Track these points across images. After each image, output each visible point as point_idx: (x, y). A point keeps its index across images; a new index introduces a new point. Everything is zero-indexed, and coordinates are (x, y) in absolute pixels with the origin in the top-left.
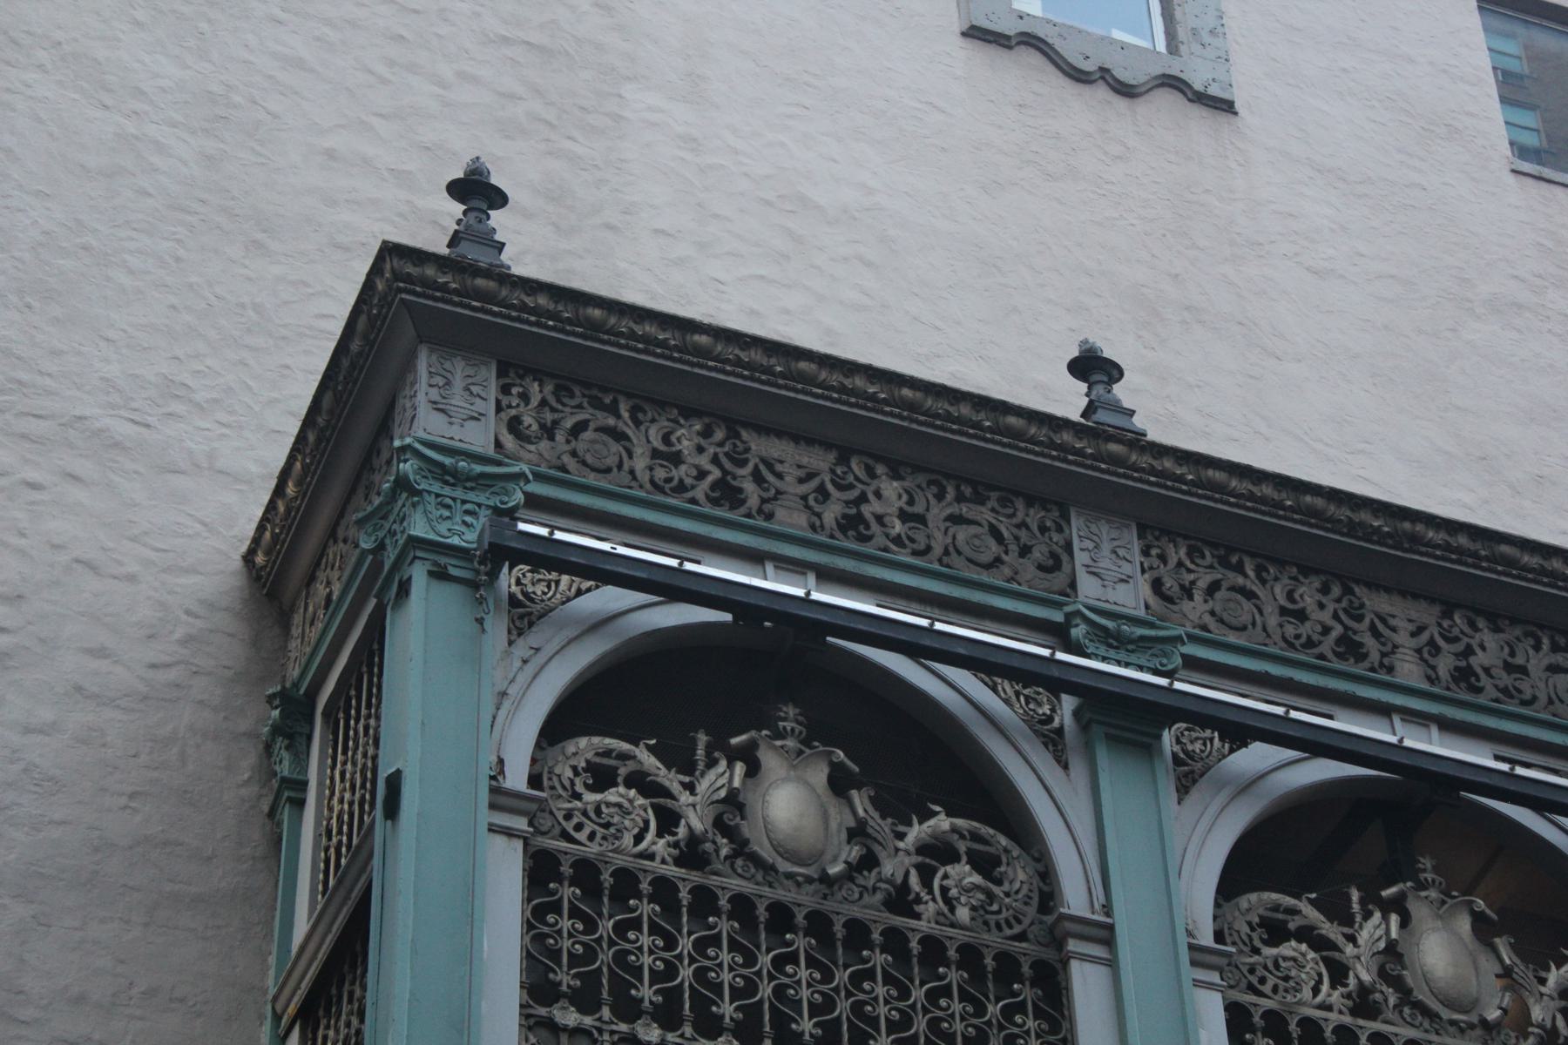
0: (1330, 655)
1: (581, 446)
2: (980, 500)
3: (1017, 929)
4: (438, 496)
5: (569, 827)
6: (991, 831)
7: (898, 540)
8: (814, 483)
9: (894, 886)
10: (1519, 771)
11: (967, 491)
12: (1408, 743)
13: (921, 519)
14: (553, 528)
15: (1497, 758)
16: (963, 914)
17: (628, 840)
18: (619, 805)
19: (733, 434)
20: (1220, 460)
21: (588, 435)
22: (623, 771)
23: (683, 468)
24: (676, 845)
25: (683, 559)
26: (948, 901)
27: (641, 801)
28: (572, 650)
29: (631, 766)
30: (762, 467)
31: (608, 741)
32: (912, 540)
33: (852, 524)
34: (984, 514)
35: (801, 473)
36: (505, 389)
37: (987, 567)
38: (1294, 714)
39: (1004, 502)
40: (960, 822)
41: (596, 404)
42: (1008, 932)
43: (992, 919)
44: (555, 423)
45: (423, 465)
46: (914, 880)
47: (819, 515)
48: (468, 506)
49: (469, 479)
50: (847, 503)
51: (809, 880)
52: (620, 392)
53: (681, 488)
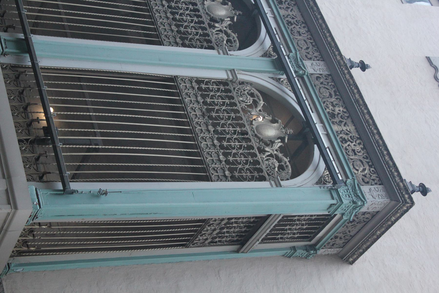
0: (290, 29)
3: (270, 174)
5: (236, 89)
6: (290, 169)
7: (346, 149)
8: (349, 133)
10: (277, 36)
11: (370, 164)
12: (317, 125)
15: (275, 28)
16: (267, 162)
17: (241, 99)
18: (247, 97)
19: (348, 117)
21: (327, 91)
22: (255, 98)
23: (332, 107)
24: (245, 108)
25: (307, 99)
26: (267, 160)
27: (251, 102)
28: (271, 80)
29: (258, 100)
32: (349, 152)
33: (344, 140)
34: (367, 168)
35: (349, 130)
36: (325, 76)
38: (306, 102)
40: (288, 163)
41: (335, 92)
42: (268, 172)
44: (325, 84)
45: (353, 184)
46: (267, 154)
47: (341, 133)
49: (356, 194)
50: (348, 139)
51: (254, 132)
52: (308, 26)
53: (328, 107)
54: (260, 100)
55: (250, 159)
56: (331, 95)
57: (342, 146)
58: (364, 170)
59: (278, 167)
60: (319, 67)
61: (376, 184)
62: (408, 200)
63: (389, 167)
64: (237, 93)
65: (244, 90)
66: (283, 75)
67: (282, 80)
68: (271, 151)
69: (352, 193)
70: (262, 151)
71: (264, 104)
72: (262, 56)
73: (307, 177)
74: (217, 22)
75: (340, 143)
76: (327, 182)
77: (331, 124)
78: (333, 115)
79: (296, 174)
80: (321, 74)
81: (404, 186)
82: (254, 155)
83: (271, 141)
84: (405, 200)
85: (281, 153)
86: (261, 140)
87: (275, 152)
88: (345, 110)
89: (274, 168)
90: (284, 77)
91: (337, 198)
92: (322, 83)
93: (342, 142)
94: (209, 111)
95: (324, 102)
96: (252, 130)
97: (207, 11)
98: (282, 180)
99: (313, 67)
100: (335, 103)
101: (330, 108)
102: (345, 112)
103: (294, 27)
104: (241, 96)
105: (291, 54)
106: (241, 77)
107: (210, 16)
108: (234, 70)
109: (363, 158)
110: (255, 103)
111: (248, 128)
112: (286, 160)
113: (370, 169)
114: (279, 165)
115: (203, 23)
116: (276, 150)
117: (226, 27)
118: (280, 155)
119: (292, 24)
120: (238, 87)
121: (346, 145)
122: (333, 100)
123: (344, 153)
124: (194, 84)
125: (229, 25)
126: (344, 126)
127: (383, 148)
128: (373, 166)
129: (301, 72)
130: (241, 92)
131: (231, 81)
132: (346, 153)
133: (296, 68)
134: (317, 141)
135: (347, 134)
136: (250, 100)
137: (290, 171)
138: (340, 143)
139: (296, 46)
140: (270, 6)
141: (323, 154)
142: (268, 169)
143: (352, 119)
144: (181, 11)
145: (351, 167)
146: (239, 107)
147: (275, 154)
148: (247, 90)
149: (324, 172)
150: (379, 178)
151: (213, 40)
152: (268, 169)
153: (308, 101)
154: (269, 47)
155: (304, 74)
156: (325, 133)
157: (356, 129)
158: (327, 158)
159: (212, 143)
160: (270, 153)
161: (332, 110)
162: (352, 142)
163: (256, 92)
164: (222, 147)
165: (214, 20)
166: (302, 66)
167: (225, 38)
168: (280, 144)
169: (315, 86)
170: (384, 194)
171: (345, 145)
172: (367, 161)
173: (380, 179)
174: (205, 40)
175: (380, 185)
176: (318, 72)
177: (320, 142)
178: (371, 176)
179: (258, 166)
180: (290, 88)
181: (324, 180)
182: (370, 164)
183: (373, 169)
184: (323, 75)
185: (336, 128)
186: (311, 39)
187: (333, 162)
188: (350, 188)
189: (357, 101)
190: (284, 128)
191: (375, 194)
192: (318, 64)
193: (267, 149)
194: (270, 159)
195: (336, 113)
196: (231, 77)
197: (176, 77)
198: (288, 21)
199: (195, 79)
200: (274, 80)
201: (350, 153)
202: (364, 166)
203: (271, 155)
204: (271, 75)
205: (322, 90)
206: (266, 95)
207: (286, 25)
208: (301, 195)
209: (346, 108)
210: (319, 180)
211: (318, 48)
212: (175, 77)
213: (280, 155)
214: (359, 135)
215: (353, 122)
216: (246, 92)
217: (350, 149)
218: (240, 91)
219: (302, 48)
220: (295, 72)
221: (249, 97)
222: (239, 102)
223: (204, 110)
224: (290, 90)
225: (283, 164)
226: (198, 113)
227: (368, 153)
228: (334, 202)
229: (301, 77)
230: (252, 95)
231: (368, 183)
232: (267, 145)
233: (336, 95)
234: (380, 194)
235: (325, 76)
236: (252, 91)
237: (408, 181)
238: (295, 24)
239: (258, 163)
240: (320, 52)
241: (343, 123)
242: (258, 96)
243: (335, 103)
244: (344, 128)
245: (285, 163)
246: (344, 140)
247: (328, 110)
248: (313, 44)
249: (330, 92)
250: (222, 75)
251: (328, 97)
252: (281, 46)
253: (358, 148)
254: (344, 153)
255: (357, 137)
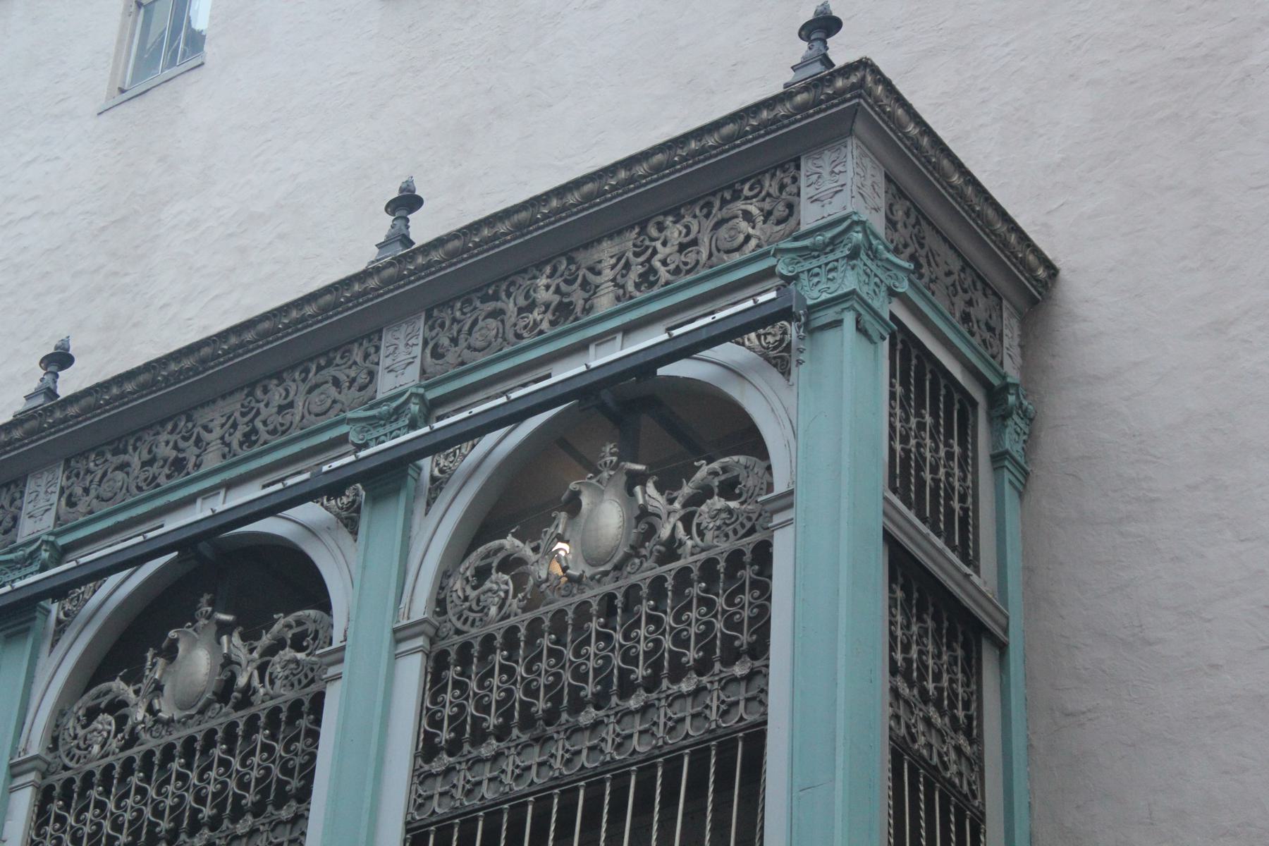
1: (472, 341)
2: (737, 196)
3: (748, 525)
4: (809, 271)
5: (459, 625)
6: (735, 458)
7: (677, 271)
8: (623, 261)
9: (662, 544)
10: (290, 482)
11: (728, 196)
12: (593, 364)
13: (695, 242)
14: (75, 560)
15: (264, 487)
16: (709, 536)
18: (490, 590)
19: (571, 261)
20: (139, 368)
21: (481, 324)
22: (495, 565)
23: (536, 313)
25: (504, 393)
26: (701, 534)
27: (506, 577)
29: (501, 556)
30: (650, 251)
31: (480, 550)
32: (686, 264)
33: (648, 277)
34: (740, 205)
35: (613, 261)
36: (432, 328)
37: (739, 249)
38: (514, 395)
39: (101, 454)
40: (716, 465)
41: (485, 299)
42: (741, 532)
43: (729, 530)
44: (459, 331)
46: (681, 532)
47: (623, 287)
48: (830, 266)
50: (642, 264)
51: (606, 574)
53: (536, 324)
54: (501, 548)
55: (696, 590)
56: (497, 314)
57: (667, 283)
58: (747, 216)
59: (728, 499)
60: (402, 347)
61: (795, 180)
62: (853, 79)
63: (741, 134)
64: (473, 625)
65: (466, 599)
66: (420, 469)
67: (436, 472)
68: (672, 520)
69: (823, 260)
70: (671, 550)
71: (515, 535)
72: (354, 533)
73: (763, 403)
74: (233, 678)
75: (656, 290)
76: (782, 341)
77: (592, 316)
78: (563, 310)
79: (749, 439)
80: (426, 343)
81: (806, 89)
82: (683, 576)
83: (639, 519)
84: (853, 87)
85: (680, 487)
86: (635, 551)
87: (677, 505)
88: (548, 270)
89: (730, 511)
90: (426, 463)
91: (838, 308)
92: (454, 341)
93: (652, 285)
94: (528, 721)
95: (519, 337)
96: (599, 581)
97: (193, 711)
98: (770, 488)
99: (400, 367)
100: (522, 302)
101: (538, 318)
102: (555, 270)
103: (265, 423)
104: (484, 610)
105: (353, 437)
106: (420, 608)
107: (209, 704)
108: (395, 631)
109: (707, 216)
110: (511, 564)
111: (592, 594)
112: (703, 471)
113: (747, 198)
114: (720, 495)
115: (233, 725)
116: (671, 501)
117: (251, 651)
118: (687, 489)
119: (254, 431)
120: (454, 619)
121: (662, 271)
122: (511, 308)
123: (690, 277)
124: (436, 766)
125: (244, 638)
126: (599, 273)
127: (679, 152)
128: (737, 186)
129: (414, 408)
130: (470, 609)
131: (432, 642)
132: (688, 272)
133: (401, 424)
134: (644, 367)
135: (627, 266)
136: (500, 581)
137: (742, 459)
138: (656, 290)
139: (328, 421)
140: (189, 501)
141: (689, 349)
142: (731, 534)
143: (577, 249)
144: (189, 798)
145: (737, 257)
146: (521, 620)
147: (684, 506)
148: (464, 591)
149: (749, 348)
150: (776, 168)
151: (291, 695)
152: (731, 534)
153: (512, 390)
154: (327, 508)
155: (422, 397)
156: (619, 337)
157: (611, 237)
158: (704, 335)
159: (637, 718)
160: (680, 525)
161: (545, 312)
162: (655, 252)
163: (474, 559)
164: (651, 684)
165: (224, 691)
166: (394, 404)
167: (288, 653)
168: (651, 489)
169: (463, 363)
170: (828, 156)
171: (663, 274)
172: (717, 204)
173: (782, 167)
174: (291, 721)
175: (798, 168)
176: (417, 351)
177: (650, 357)
178: (768, 195)
179: (721, 567)
180: (465, 447)
181: (775, 348)
182: (728, 196)
183: (747, 187)
184: (428, 334)
185: (605, 303)
186: (307, 371)
187: (719, 316)
188: (807, 265)
189: (520, 228)
190: (597, 472)
191: (828, 184)
192: (391, 349)
193: (665, 533)
194: (699, 525)
195: (557, 298)
196: (420, 642)
197: (409, 827)
198: (241, 444)
199: (420, 761)
200: (434, 499)
201: (691, 258)
202: (736, 217)
203: (687, 520)
204: (420, 506)
205: (477, 339)
206: (484, 526)
207: (256, 449)
208: (824, 431)
209: (539, 266)
210: (775, 366)
211: (336, 350)
212: (408, 831)
213: (687, 489)
214: (632, 227)
215: (587, 246)
216: (473, 594)
217: (675, 260)
218: (466, 613)
219: (334, 402)
220: (413, 426)
221: (488, 585)
222: (503, 619)
223: (525, 738)
224: (474, 446)
225: (716, 482)
226: (534, 757)
227: (693, 203)
228: (849, 320)
229: (431, 408)
230: (482, 574)
231: (790, 207)
232: (652, 531)
233: (496, 297)
234: (828, 169)
235: (432, 328)
236: (468, 573)
237: (790, 76)
238: (252, 420)
239: (709, 568)
240: (352, 342)
241: (590, 277)
242: (487, 556)
243: (522, 302)
244: (608, 274)
245: (715, 474)
246: (648, 277)
247: (545, 326)
248: (323, 362)
249: (484, 314)
250: (412, 670)
251: (503, 321)
252: (325, 468)
253: (675, 233)
254: (690, 277)
255: (639, 234)
